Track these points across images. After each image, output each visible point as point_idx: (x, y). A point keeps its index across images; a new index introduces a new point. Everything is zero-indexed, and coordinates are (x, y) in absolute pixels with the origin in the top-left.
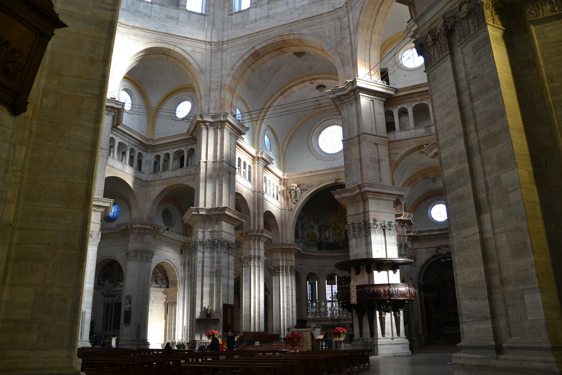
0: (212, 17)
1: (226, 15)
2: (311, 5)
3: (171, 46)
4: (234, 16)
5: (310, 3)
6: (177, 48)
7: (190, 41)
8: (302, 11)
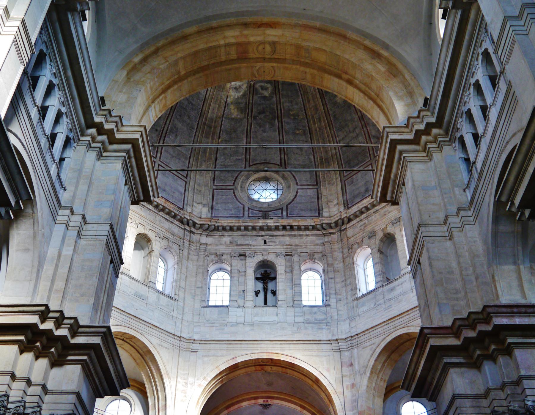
0: (182, 304)
1: (198, 305)
2: (306, 325)
3: (138, 334)
4: (206, 309)
5: (305, 322)
6: (144, 338)
7: (159, 331)
8: (295, 329)
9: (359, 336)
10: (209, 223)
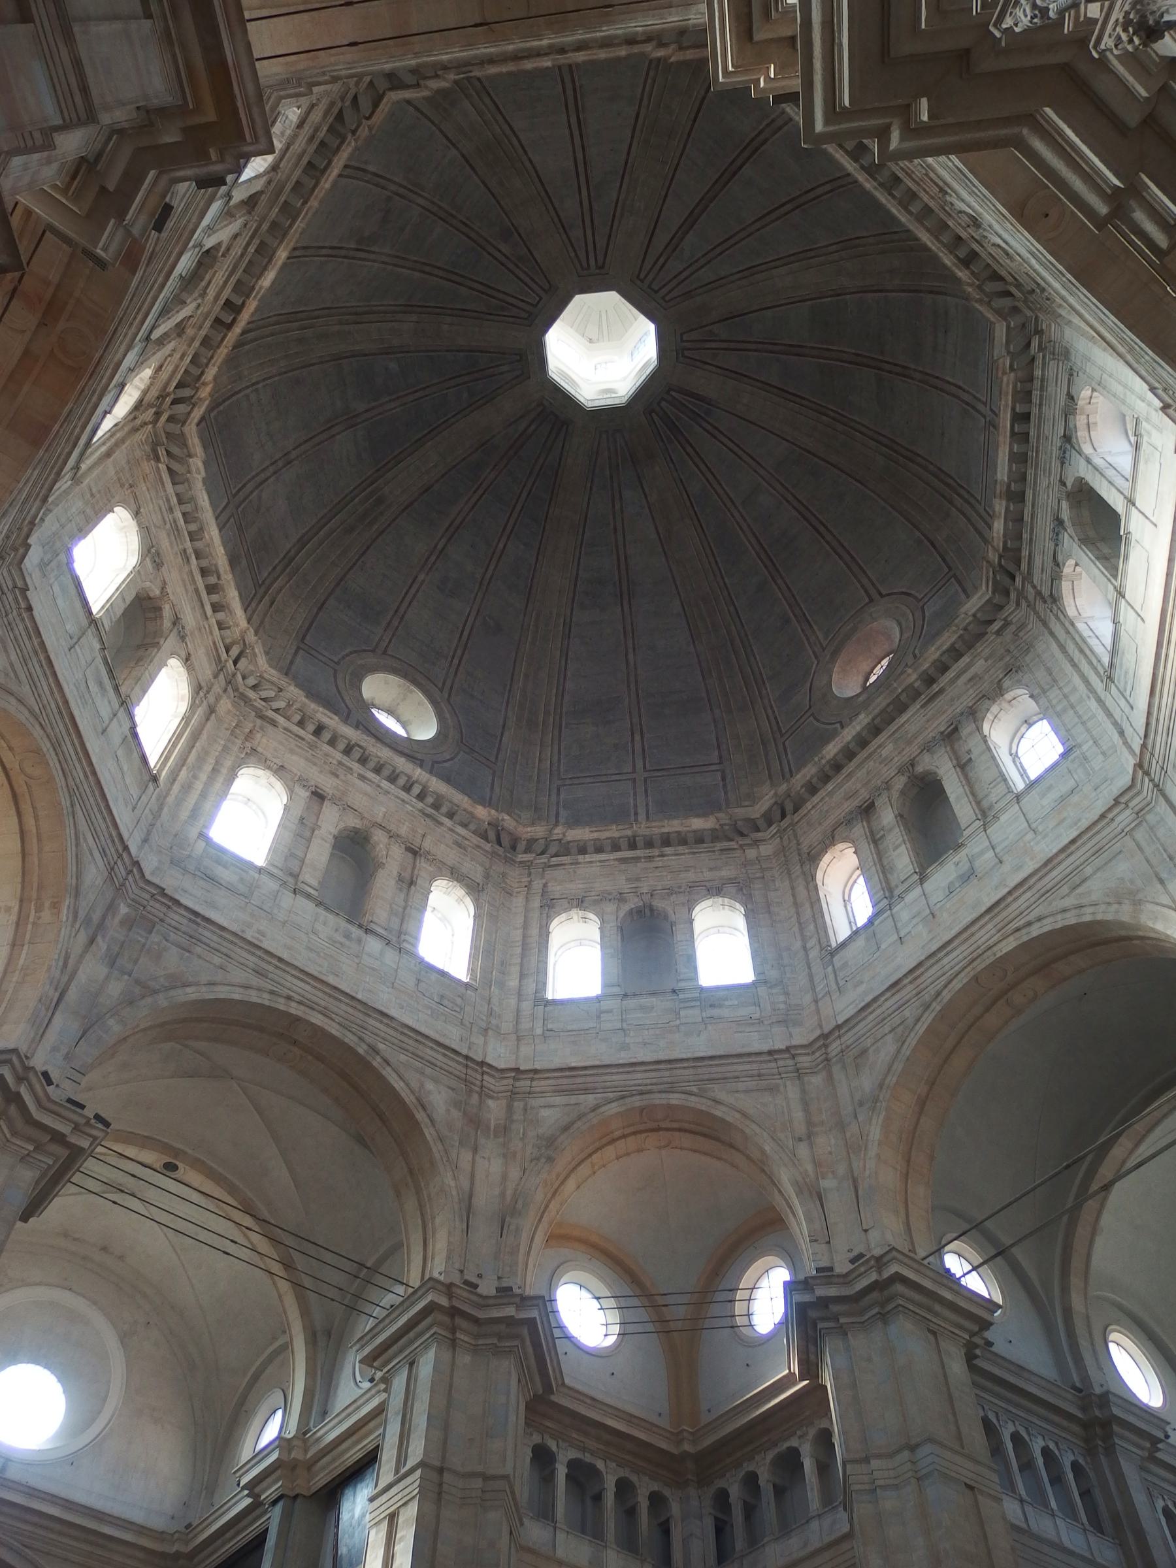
9: (25, 615)
10: (369, 122)
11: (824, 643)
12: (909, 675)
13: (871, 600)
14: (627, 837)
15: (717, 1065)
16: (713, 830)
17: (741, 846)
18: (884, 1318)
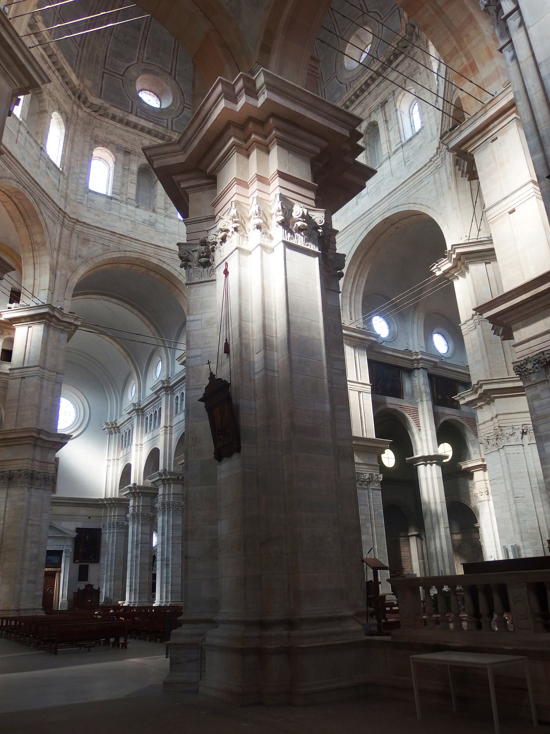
11: (144, 61)
12: (175, 135)
13: (170, 74)
14: (53, 52)
15: (47, 199)
16: (75, 86)
17: (75, 101)
18: (62, 331)
